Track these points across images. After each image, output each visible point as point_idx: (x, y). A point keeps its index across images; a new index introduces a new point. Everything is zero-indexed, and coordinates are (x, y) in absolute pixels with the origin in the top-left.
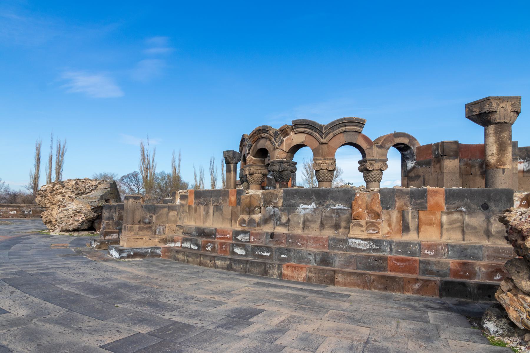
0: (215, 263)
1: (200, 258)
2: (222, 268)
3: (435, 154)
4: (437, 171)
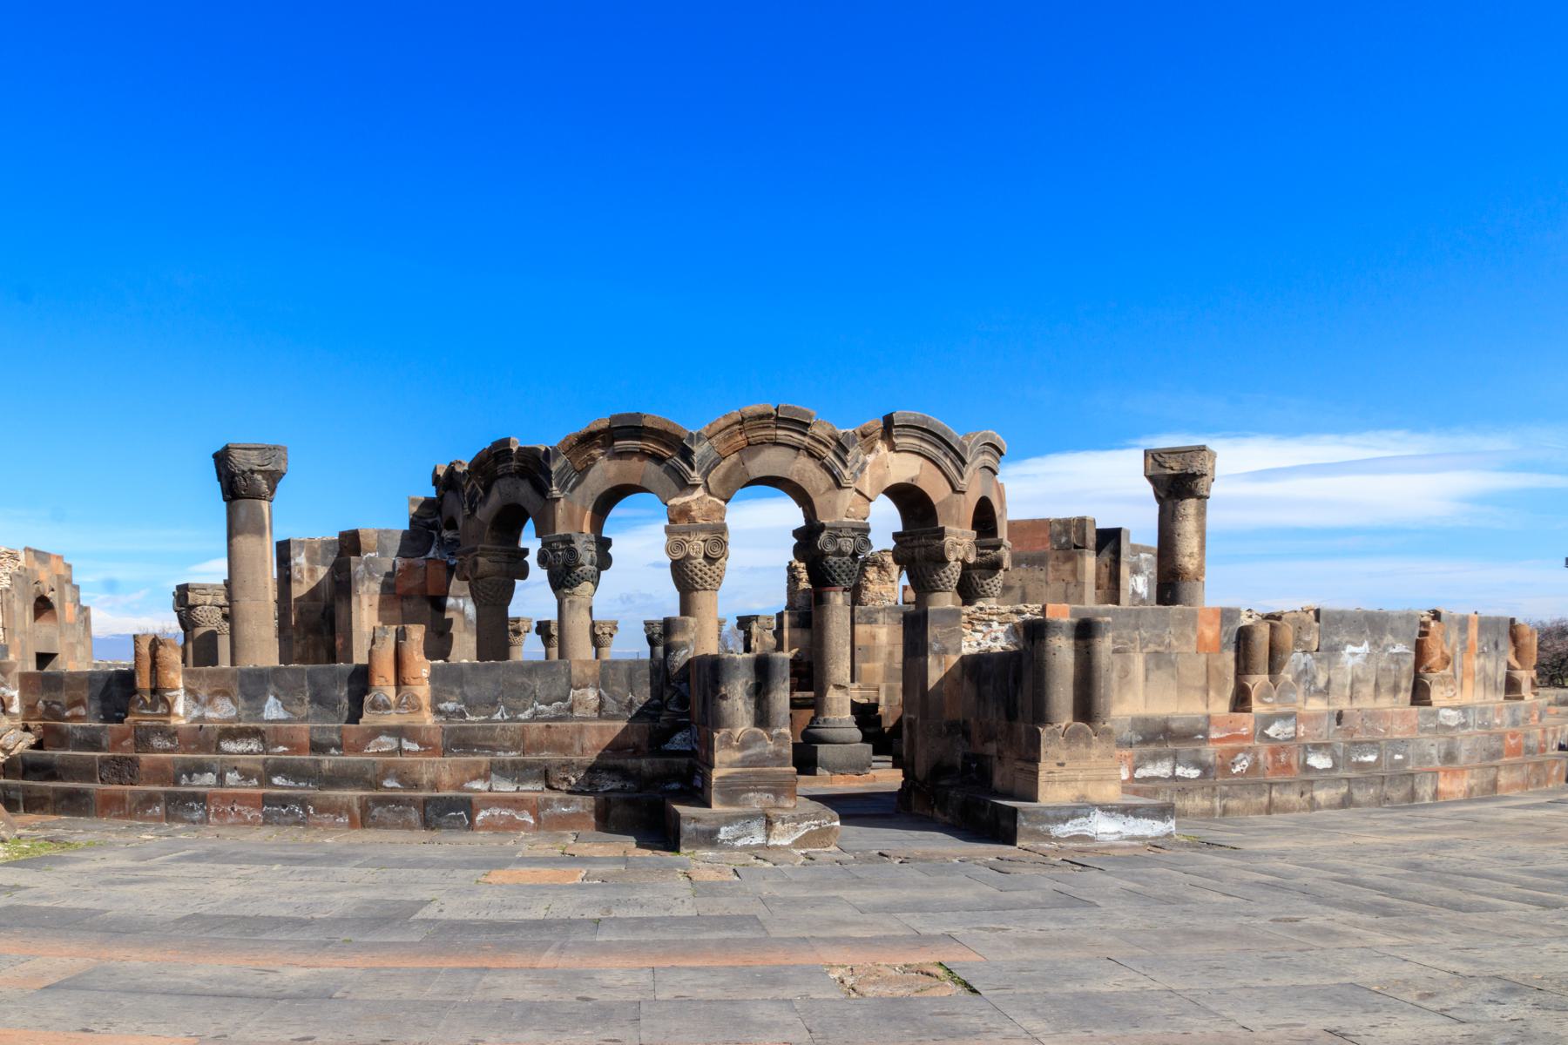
0: (1312, 798)
1: (1270, 793)
2: (1330, 807)
3: (1058, 542)
4: (1064, 577)
